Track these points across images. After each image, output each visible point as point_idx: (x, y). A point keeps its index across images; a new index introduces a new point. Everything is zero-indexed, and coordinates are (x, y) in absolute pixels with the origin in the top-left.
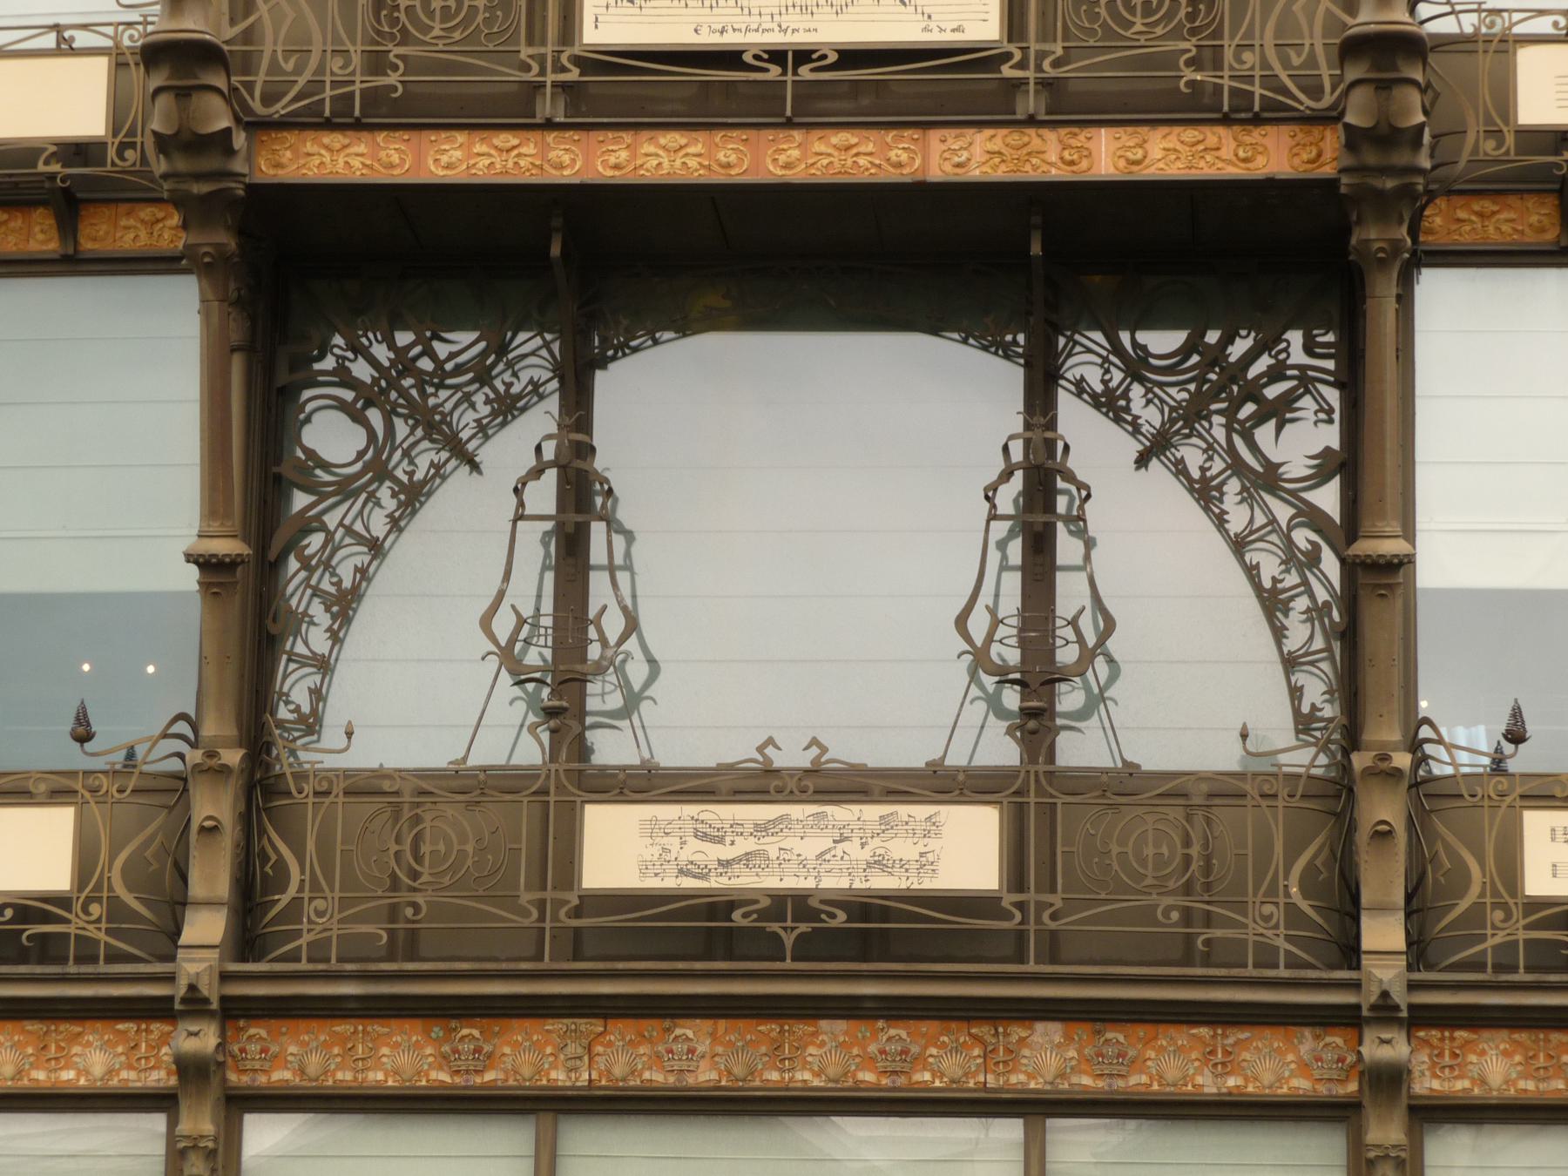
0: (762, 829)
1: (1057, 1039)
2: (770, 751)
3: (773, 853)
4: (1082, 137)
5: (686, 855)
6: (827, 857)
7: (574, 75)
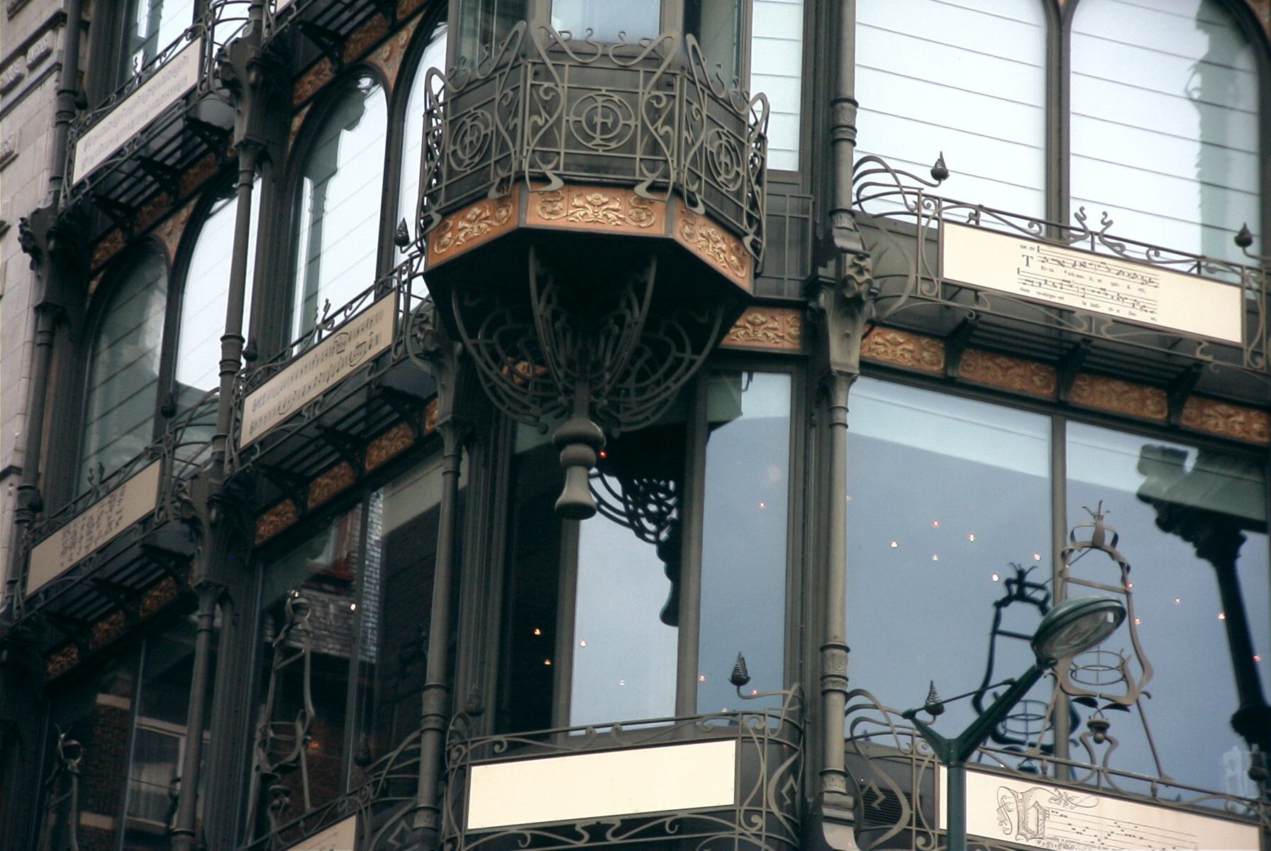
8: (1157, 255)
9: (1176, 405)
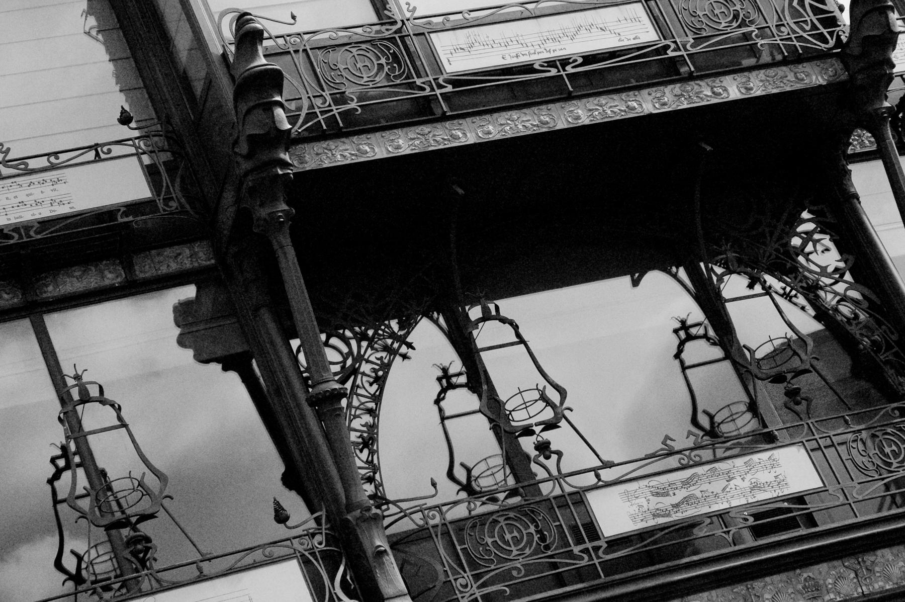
0: (686, 483)
1: (891, 558)
2: (669, 442)
3: (699, 495)
4: (718, 81)
5: (652, 506)
6: (728, 490)
7: (449, 88)
8: (57, 158)
9: (129, 267)
